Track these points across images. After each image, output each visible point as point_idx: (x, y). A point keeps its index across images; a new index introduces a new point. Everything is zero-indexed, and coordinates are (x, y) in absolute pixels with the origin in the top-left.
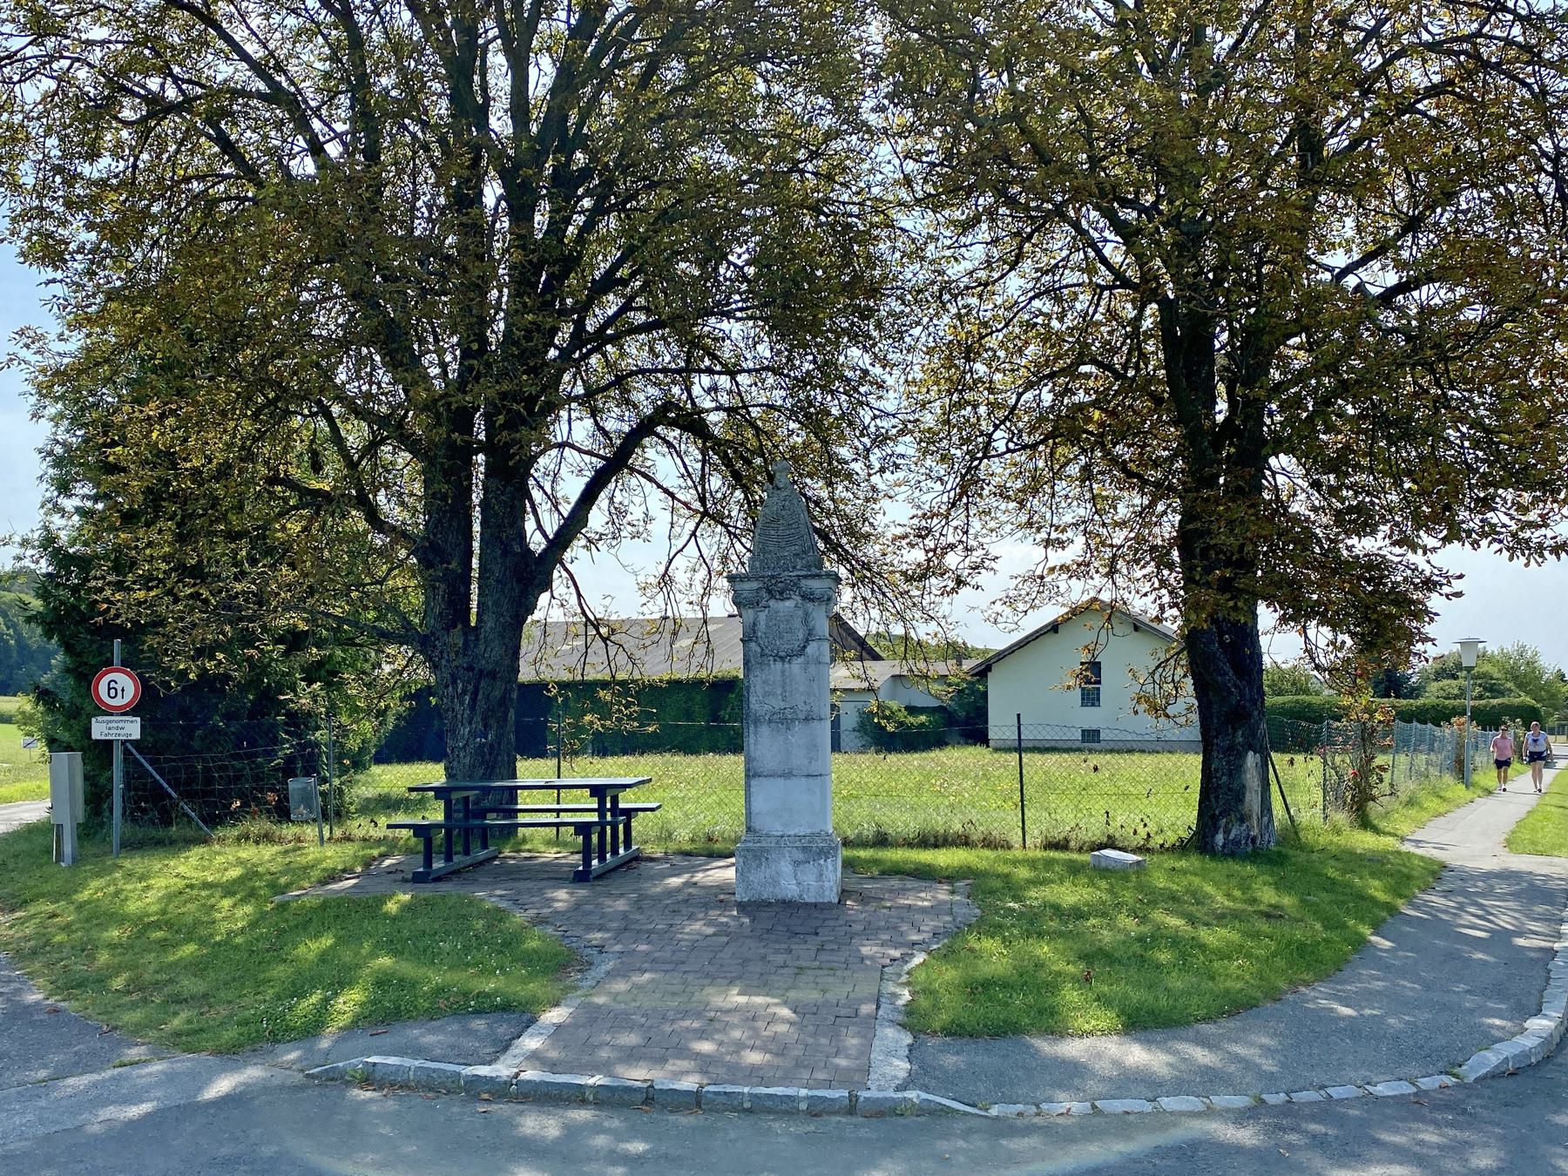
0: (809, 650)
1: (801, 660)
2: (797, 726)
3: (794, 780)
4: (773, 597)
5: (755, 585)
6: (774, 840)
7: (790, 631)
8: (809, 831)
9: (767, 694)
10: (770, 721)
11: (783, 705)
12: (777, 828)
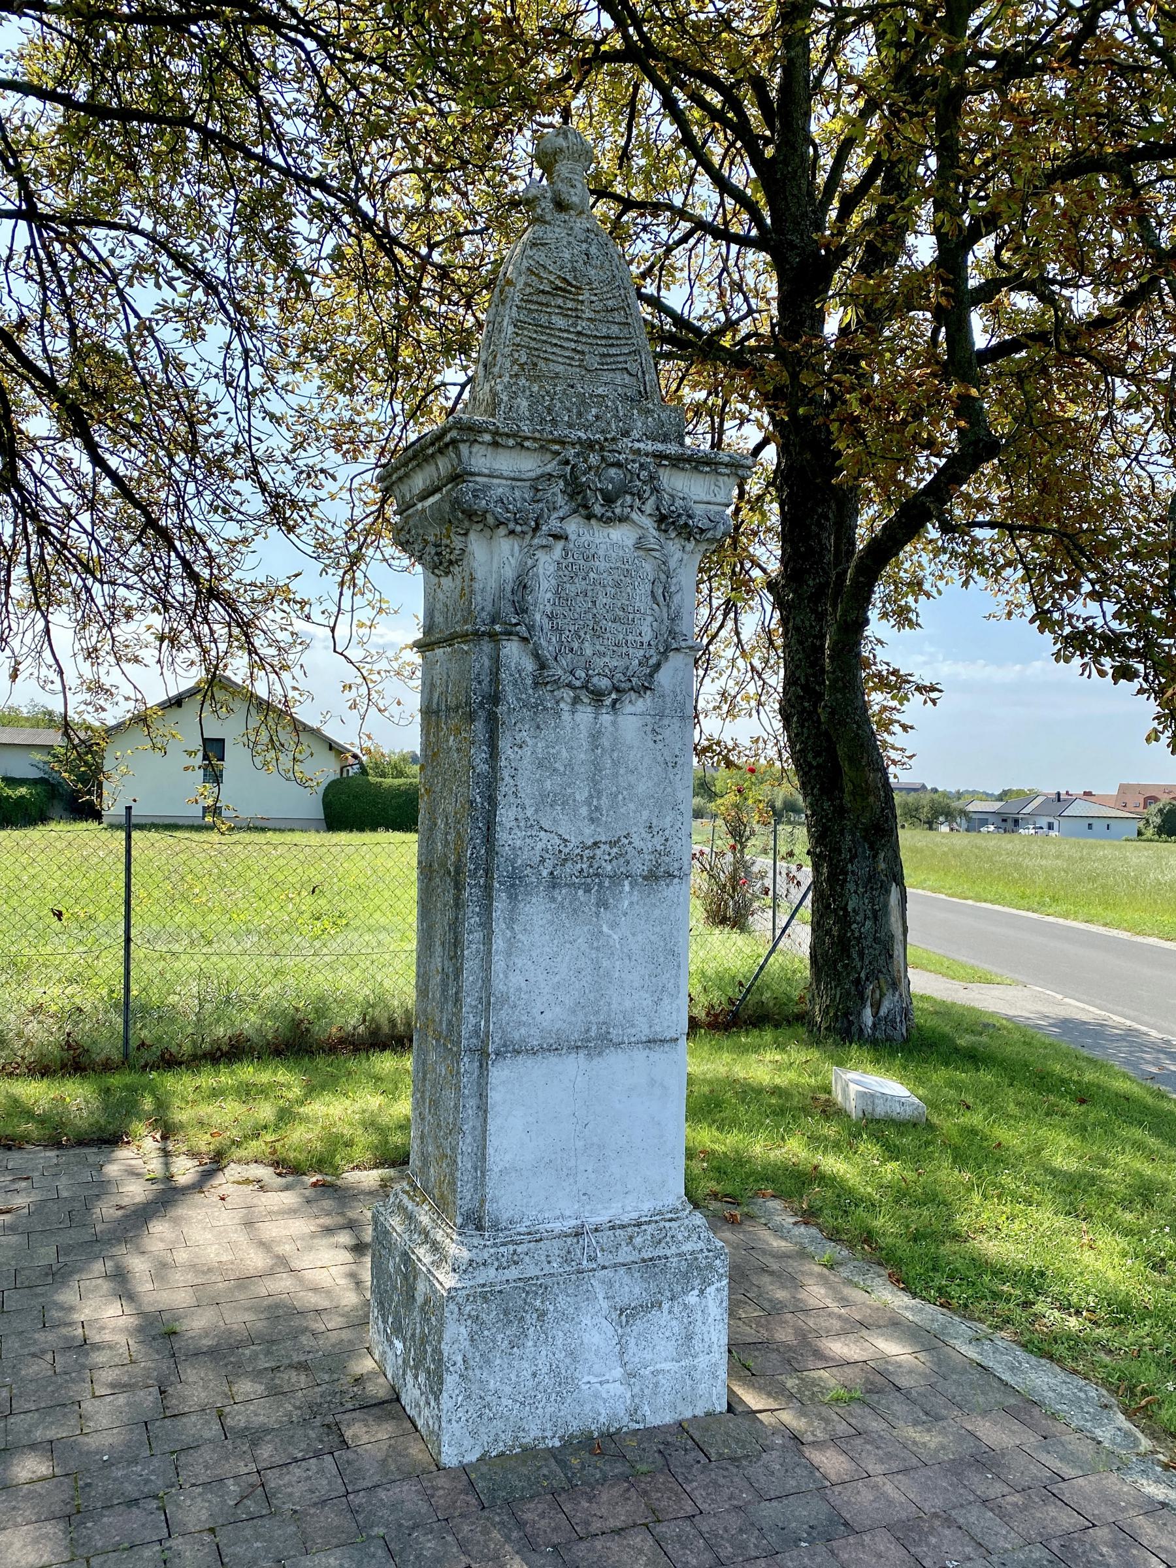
0: (664, 677)
1: (642, 704)
2: (628, 897)
3: (614, 1060)
5: (528, 464)
6: (555, 1247)
7: (625, 617)
8: (647, 1206)
9: (546, 800)
10: (554, 883)
11: (589, 833)
12: (560, 1210)
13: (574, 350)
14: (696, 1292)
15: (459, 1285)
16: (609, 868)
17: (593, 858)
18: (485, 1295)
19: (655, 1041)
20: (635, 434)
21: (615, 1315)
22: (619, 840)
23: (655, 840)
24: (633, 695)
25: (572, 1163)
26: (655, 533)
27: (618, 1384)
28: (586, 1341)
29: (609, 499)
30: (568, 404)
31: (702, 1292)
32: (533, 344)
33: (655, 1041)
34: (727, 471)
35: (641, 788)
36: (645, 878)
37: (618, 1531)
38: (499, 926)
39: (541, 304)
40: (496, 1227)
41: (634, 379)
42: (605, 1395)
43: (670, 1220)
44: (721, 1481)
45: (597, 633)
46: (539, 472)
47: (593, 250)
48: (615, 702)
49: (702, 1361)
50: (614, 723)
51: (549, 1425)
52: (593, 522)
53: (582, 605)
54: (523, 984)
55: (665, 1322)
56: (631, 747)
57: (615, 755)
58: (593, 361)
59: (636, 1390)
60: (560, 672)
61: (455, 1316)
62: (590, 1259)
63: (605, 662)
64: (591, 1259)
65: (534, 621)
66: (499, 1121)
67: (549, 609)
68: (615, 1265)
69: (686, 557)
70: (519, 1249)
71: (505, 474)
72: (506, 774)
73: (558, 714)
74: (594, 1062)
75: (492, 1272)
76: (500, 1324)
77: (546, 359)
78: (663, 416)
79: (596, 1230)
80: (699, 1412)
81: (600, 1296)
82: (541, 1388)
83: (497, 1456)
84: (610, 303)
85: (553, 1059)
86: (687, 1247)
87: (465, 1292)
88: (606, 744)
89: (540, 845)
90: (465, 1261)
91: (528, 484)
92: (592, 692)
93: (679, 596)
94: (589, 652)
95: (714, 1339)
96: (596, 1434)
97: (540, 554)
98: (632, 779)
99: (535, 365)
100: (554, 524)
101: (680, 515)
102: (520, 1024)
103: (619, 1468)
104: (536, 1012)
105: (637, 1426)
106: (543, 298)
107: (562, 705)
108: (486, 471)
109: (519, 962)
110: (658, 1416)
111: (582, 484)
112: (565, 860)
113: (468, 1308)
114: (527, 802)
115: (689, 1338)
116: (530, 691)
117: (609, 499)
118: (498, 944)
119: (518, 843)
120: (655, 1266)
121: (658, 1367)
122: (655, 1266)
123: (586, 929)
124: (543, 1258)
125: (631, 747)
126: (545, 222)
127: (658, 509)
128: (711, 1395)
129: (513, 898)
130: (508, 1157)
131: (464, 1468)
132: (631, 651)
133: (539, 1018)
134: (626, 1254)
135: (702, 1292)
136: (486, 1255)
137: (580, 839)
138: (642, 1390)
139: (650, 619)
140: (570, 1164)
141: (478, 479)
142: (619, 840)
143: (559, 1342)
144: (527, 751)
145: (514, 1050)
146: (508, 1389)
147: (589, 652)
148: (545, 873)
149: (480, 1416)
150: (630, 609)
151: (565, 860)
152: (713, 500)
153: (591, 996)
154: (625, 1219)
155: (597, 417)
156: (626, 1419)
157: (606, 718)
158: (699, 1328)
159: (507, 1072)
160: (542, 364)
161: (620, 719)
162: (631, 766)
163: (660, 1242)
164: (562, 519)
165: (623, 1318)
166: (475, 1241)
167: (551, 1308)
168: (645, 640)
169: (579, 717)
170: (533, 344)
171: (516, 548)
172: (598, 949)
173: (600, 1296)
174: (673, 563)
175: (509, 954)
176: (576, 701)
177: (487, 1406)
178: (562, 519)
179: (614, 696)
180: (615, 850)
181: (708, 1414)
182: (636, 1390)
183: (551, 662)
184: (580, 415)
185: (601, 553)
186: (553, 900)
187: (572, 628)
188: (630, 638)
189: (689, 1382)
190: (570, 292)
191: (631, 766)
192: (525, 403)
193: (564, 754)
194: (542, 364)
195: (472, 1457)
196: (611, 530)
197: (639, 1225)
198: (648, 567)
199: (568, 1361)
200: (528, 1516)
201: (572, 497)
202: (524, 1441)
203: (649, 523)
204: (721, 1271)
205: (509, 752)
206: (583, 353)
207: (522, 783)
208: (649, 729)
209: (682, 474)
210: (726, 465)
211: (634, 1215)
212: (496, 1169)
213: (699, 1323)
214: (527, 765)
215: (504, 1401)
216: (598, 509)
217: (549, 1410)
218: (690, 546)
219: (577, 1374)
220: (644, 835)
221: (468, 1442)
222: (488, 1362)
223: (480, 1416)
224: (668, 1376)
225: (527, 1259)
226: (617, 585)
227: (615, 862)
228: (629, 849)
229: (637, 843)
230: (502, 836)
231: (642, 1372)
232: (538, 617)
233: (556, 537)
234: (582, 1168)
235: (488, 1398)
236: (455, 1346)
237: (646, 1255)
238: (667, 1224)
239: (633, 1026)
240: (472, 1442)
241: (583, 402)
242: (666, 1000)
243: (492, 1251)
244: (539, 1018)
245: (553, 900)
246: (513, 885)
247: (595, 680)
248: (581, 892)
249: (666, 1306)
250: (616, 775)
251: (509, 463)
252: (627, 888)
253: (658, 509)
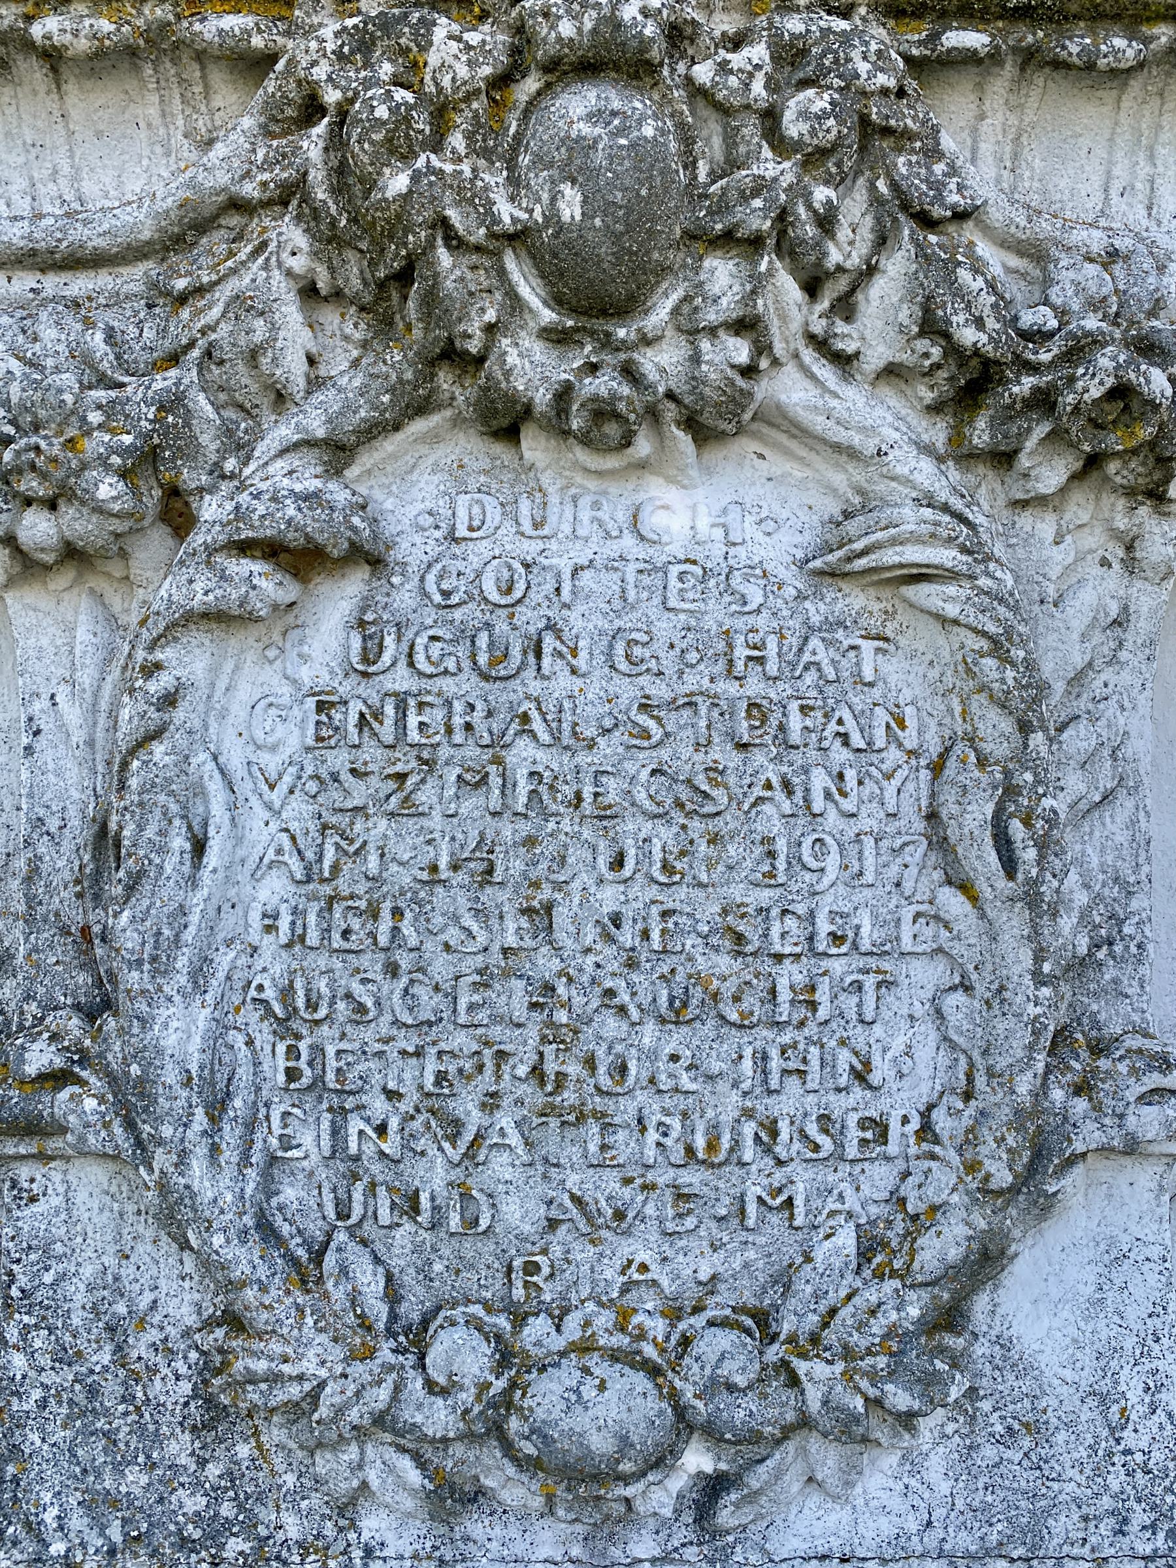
4: (448, 378)
24: (827, 1457)
26: (925, 472)
29: (595, 301)
48: (713, 1487)
52: (534, 446)
53: (459, 933)
67: (272, 965)
69: (1146, 599)
91: (133, 278)
92: (530, 1465)
93: (1114, 824)
94: (519, 1213)
97: (188, 661)
100: (278, 482)
101: (1079, 350)
107: (373, 1524)
111: (396, 223)
116: (179, 1448)
117: (595, 301)
139: (926, 975)
147: (519, 1213)
150: (784, 934)
164: (337, 452)
168: (900, 1104)
174: (1060, 649)
178: (337, 452)
179: (697, 1459)
183: (272, 1301)
185: (582, 622)
188: (790, 1102)
196: (656, 489)
198: (907, 675)
201: (381, 318)
203: (895, 428)
216: (529, 365)
226: (690, 800)
233: (300, 559)
247: (546, 1395)
253: (931, 325)
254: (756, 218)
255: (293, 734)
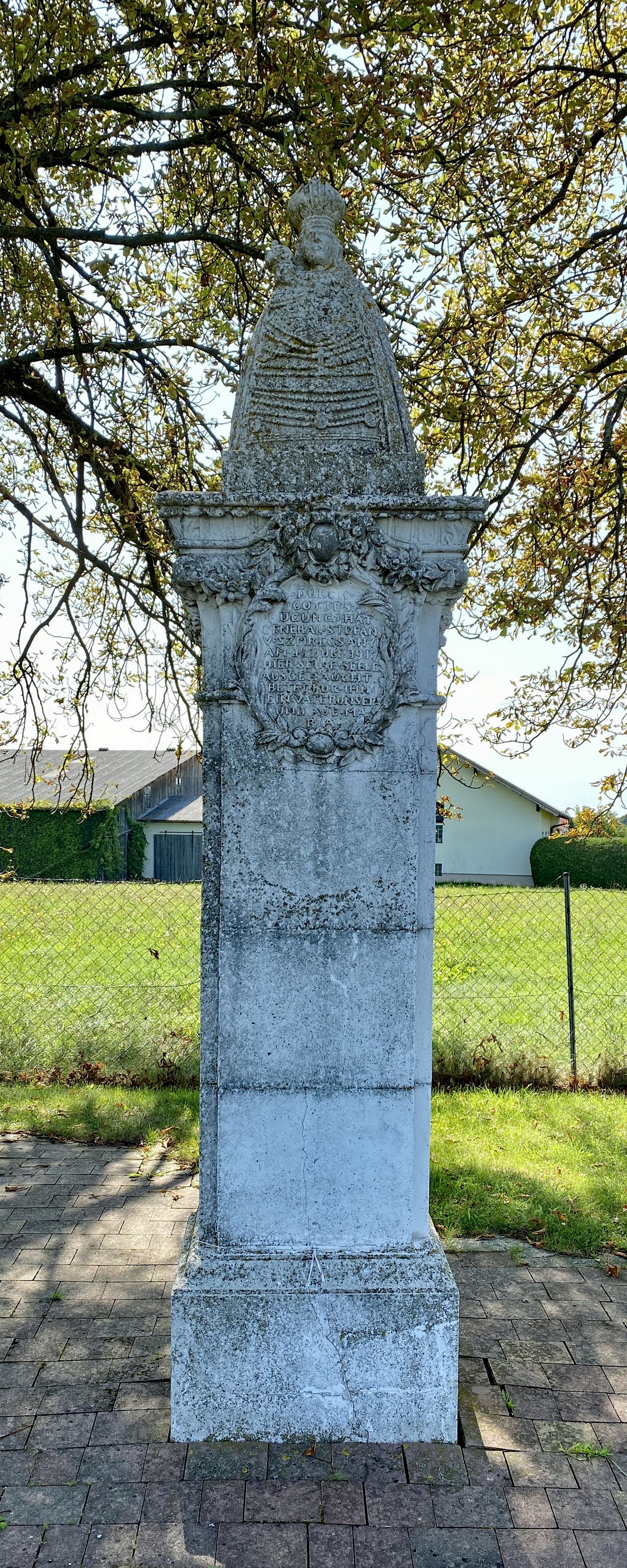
0: (395, 733)
1: (369, 761)
2: (356, 949)
3: (344, 1102)
4: (297, 570)
5: (243, 532)
6: (281, 1268)
8: (380, 1242)
9: (269, 855)
10: (279, 933)
11: (315, 887)
12: (292, 1237)
13: (305, 410)
14: (423, 1327)
15: (186, 1289)
16: (336, 920)
17: (319, 910)
18: (209, 1300)
19: (387, 1088)
20: (368, 488)
21: (336, 1336)
22: (347, 894)
23: (386, 894)
24: (358, 753)
25: (302, 1194)
26: (378, 587)
27: (339, 1399)
28: (307, 1355)
29: (323, 559)
30: (296, 467)
31: (429, 1328)
32: (268, 411)
33: (387, 1088)
34: (456, 516)
35: (370, 844)
36: (375, 931)
37: (278, 1524)
38: (225, 972)
39: (277, 368)
40: (227, 1241)
41: (374, 433)
42: (326, 1406)
43: (403, 1258)
44: (406, 1501)
45: (316, 694)
46: (252, 538)
47: (335, 304)
48: (340, 759)
49: (430, 1392)
50: (339, 781)
51: (271, 1423)
52: (312, 582)
53: (299, 665)
54: (250, 1027)
55: (389, 1350)
56: (358, 804)
57: (341, 811)
58: (323, 419)
59: (358, 1407)
60: (277, 732)
61: (181, 1314)
62: (314, 1282)
63: (329, 721)
64: (314, 1282)
65: (250, 684)
66: (229, 1149)
67: (268, 672)
68: (337, 1291)
69: (418, 610)
70: (247, 1265)
71: (218, 544)
72: (228, 831)
73: (280, 773)
74: (323, 1103)
75: (219, 1281)
76: (222, 1327)
77: (279, 424)
78: (400, 466)
79: (325, 1257)
80: (427, 1437)
81: (322, 1317)
82: (263, 1389)
83: (223, 1441)
84: (348, 355)
85: (281, 1097)
86: (416, 1285)
87: (189, 1295)
88: (332, 801)
89: (264, 899)
90: (195, 1269)
91: (243, 551)
94: (309, 712)
95: (443, 1373)
96: (318, 1439)
97: (255, 619)
98: (360, 834)
99: (269, 431)
100: (269, 588)
102: (247, 1063)
103: (320, 1472)
104: (262, 1052)
105: (360, 1440)
106: (279, 363)
107: (284, 764)
108: (199, 543)
109: (246, 1007)
110: (382, 1434)
112: (291, 912)
113: (193, 1309)
114: (251, 858)
115: (416, 1368)
116: (252, 752)
117: (323, 559)
118: (225, 988)
119: (243, 896)
120: (378, 1297)
121: (381, 1389)
122: (378, 1297)
123: (313, 978)
124: (269, 1275)
125: (358, 804)
126: (286, 284)
127: (377, 563)
128: (439, 1425)
129: (238, 946)
130: (238, 1182)
131: (188, 1445)
132: (355, 708)
133: (266, 1059)
134: (351, 1283)
135: (429, 1328)
136: (214, 1266)
137: (306, 892)
138: (364, 1408)
140: (300, 1194)
141: (193, 551)
142: (347, 894)
143: (280, 1352)
144: (250, 809)
145: (242, 1086)
146: (232, 1386)
147: (309, 712)
148: (270, 925)
149: (206, 1404)
150: (353, 667)
151: (291, 912)
152: (444, 548)
153: (319, 1041)
154: (356, 1251)
155: (327, 476)
156: (349, 1431)
157: (331, 776)
158: (425, 1360)
159: (235, 1106)
160: (275, 430)
161: (346, 775)
162: (358, 822)
163: (388, 1276)
164: (279, 583)
165: (345, 1340)
166: (209, 1253)
167: (273, 1321)
168: (372, 697)
169: (301, 775)
170: (268, 411)
171: (235, 615)
172: (325, 997)
173: (322, 1317)
174: (402, 618)
175: (235, 998)
176: (297, 760)
177: (213, 1396)
178: (279, 583)
179: (337, 753)
180: (342, 903)
181: (435, 1442)
182: (358, 1407)
184: (308, 476)
185: (320, 612)
186: (279, 950)
187: (290, 689)
188: (353, 695)
189: (415, 1409)
190: (304, 352)
191: (358, 822)
192: (251, 472)
193: (288, 811)
194: (275, 430)
195: (199, 1437)
196: (332, 589)
197: (369, 1258)
198: (376, 624)
199: (289, 1369)
200: (212, 1495)
201: (287, 559)
202: (247, 1432)
204: (450, 1311)
205: (232, 810)
206: (314, 412)
207: (245, 839)
208: (377, 785)
209: (407, 525)
210: (455, 510)
211: (367, 1249)
212: (227, 1192)
213: (426, 1356)
214: (249, 823)
215: (228, 1395)
216: (312, 570)
217: (271, 1410)
218: (422, 597)
219: (298, 1383)
220: (373, 889)
221: (195, 1424)
222: (212, 1358)
223: (206, 1404)
224: (392, 1400)
225: (253, 1274)
226: (338, 644)
227: (342, 915)
228: (358, 902)
229: (366, 897)
230: (226, 889)
231: (364, 1391)
232: (254, 680)
233: (273, 601)
234: (312, 1199)
235: (212, 1390)
236: (182, 1340)
237: (370, 1286)
238: (398, 1261)
239: (363, 1072)
240: (199, 1424)
241: (312, 463)
242: (399, 1050)
243: (221, 1263)
244: (266, 1059)
245: (279, 950)
246: (237, 935)
248: (307, 943)
249: (390, 1336)
250: (342, 831)
251: (221, 532)
252: (356, 940)
253: (377, 563)
254: (348, 547)
255: (271, 632)
